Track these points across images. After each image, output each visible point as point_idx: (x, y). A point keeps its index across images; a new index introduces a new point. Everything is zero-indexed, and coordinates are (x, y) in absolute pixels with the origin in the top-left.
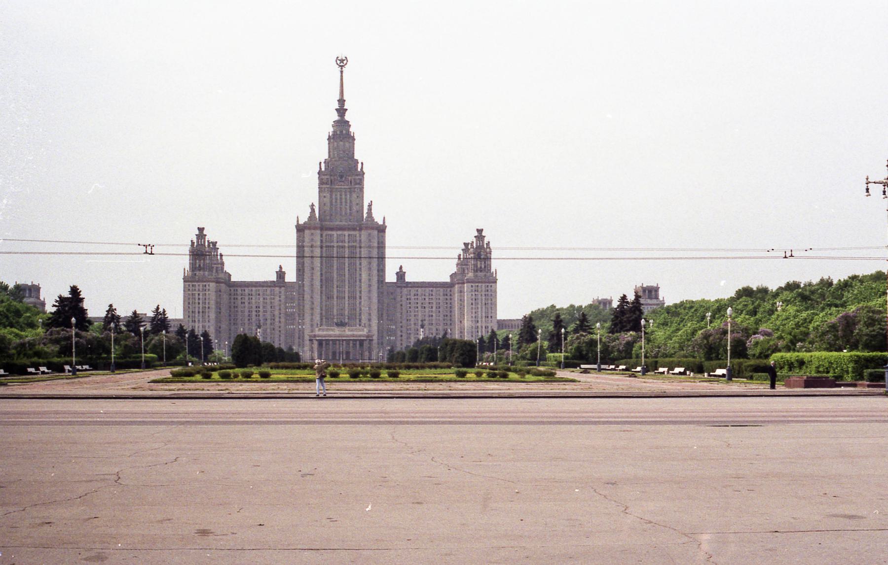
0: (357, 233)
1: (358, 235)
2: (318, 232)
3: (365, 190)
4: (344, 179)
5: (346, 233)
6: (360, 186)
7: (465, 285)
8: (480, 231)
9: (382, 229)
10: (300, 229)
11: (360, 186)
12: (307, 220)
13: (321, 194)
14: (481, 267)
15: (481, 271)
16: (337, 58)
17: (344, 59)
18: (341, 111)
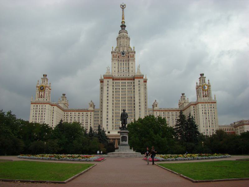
0: (132, 81)
1: (133, 83)
2: (112, 80)
3: (136, 60)
4: (124, 55)
5: (127, 81)
6: (133, 58)
7: (197, 105)
8: (202, 75)
9: (145, 81)
10: (102, 81)
11: (133, 58)
12: (105, 74)
13: (113, 63)
14: (206, 94)
15: (206, 96)
16: (121, 5)
17: (124, 5)
18: (123, 26)
